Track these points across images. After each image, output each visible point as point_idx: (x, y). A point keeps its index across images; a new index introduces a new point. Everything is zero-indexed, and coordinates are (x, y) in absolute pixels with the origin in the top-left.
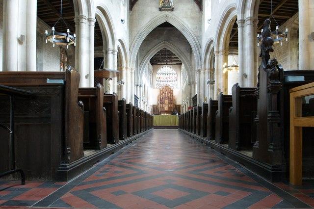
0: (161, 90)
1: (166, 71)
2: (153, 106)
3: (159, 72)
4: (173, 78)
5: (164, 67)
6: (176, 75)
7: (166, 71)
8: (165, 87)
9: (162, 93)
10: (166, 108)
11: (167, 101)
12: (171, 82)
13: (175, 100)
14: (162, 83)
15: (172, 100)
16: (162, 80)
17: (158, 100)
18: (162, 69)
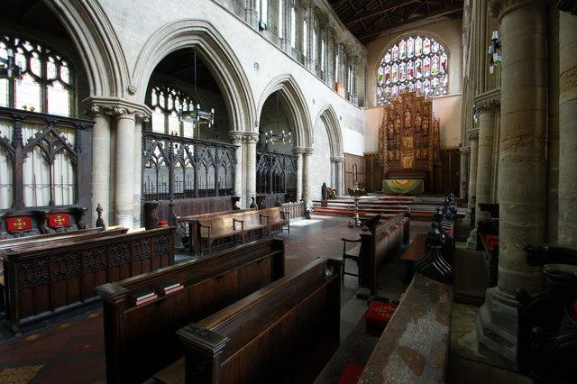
0: (388, 109)
1: (410, 50)
2: (367, 157)
3: (387, 58)
4: (435, 66)
5: (403, 43)
6: (443, 58)
7: (410, 50)
8: (403, 96)
9: (392, 115)
10: (407, 161)
11: (410, 139)
12: (427, 81)
13: (438, 134)
14: (395, 90)
15: (427, 133)
16: (395, 81)
17: (381, 139)
18: (395, 48)
